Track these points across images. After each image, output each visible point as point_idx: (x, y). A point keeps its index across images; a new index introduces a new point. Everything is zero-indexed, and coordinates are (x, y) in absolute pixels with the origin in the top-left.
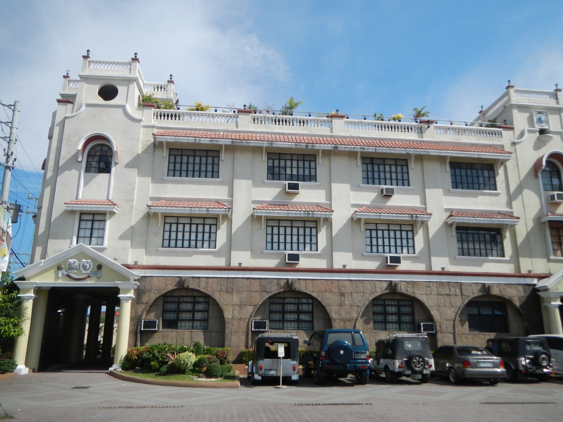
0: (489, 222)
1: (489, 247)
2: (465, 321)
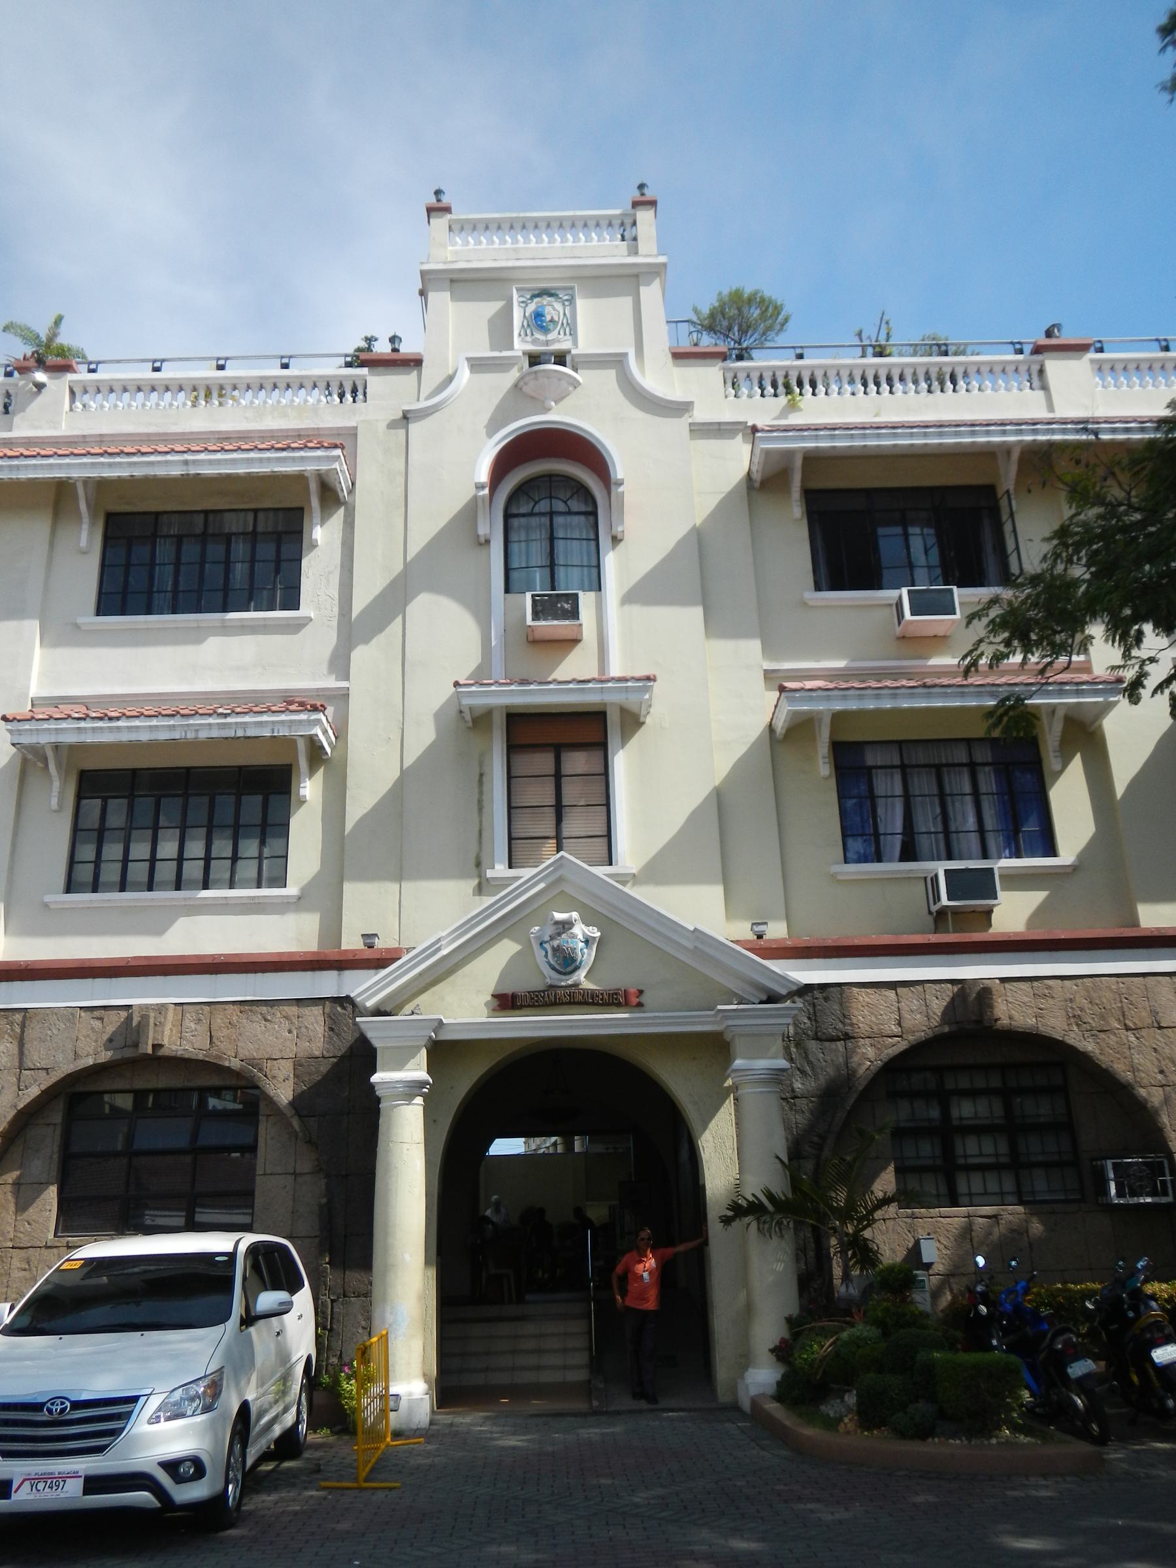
0: (177, 735)
1: (222, 847)
2: (42, 1185)
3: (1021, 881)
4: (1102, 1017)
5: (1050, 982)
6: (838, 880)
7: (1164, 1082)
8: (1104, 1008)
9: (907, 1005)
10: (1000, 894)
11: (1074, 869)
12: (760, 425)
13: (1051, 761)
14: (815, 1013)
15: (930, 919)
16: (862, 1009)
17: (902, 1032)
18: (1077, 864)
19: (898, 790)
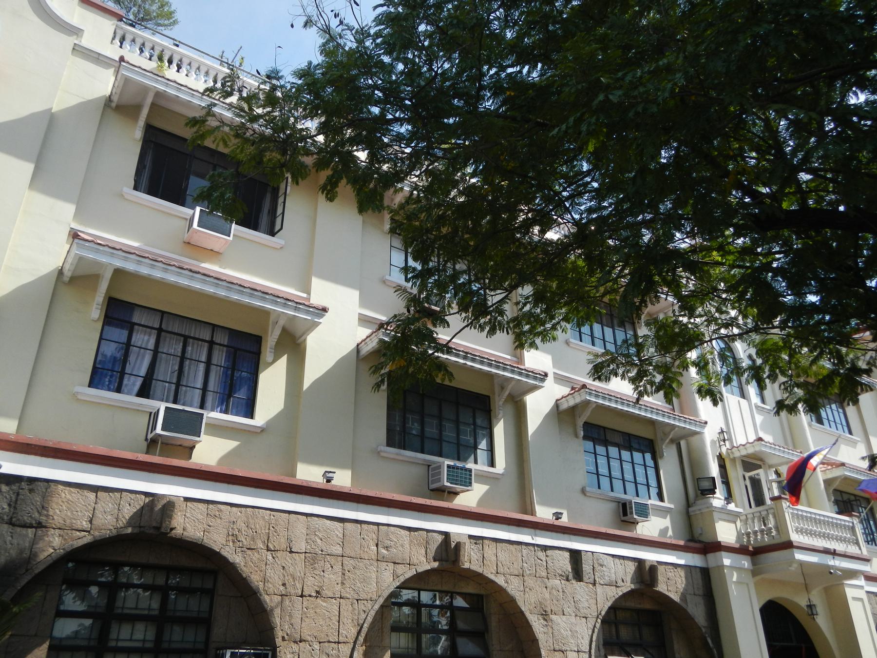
3: (220, 430)
4: (253, 539)
5: (222, 507)
6: (78, 399)
7: (283, 593)
8: (256, 532)
9: (103, 507)
10: (203, 435)
11: (263, 430)
12: (126, 59)
13: (267, 354)
14: (17, 500)
15: (145, 444)
16: (61, 504)
17: (91, 528)
18: (265, 427)
19: (151, 345)
